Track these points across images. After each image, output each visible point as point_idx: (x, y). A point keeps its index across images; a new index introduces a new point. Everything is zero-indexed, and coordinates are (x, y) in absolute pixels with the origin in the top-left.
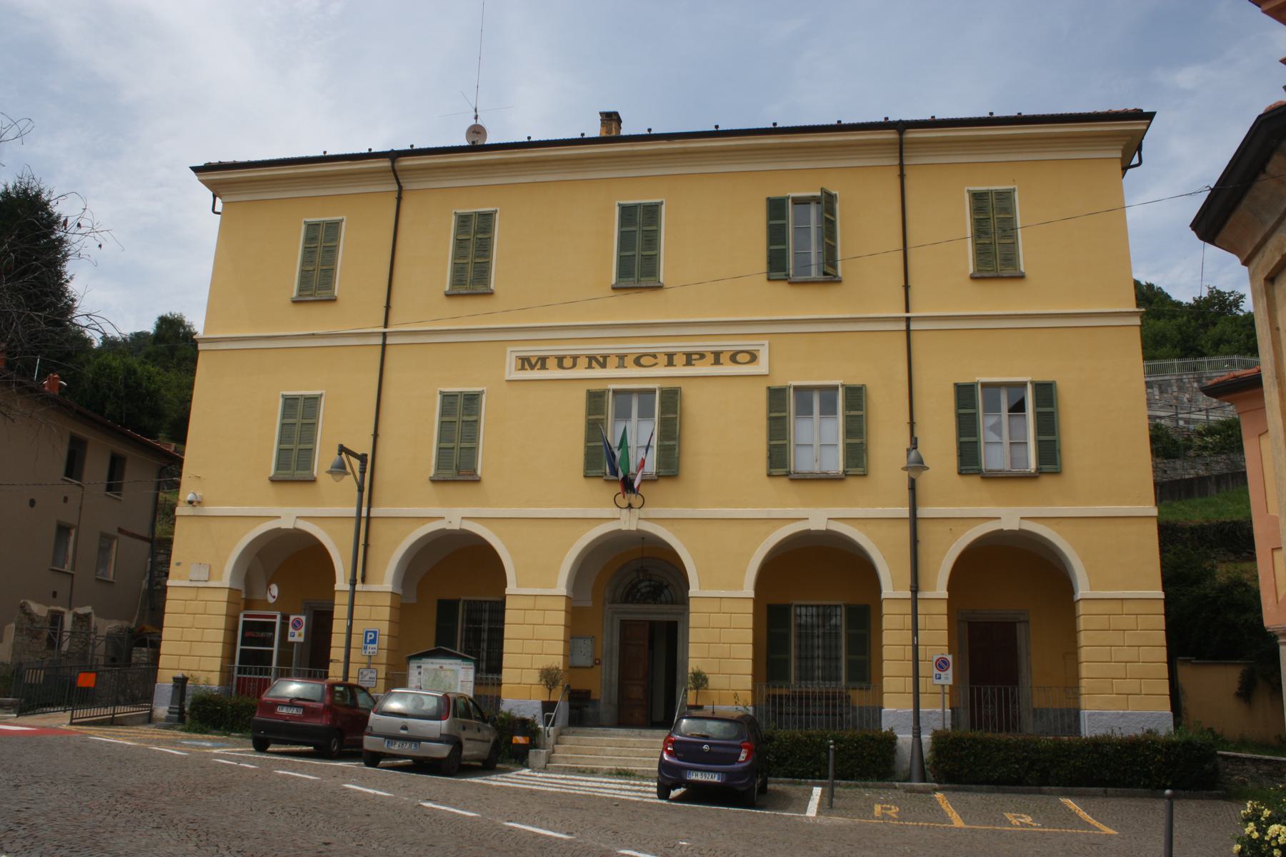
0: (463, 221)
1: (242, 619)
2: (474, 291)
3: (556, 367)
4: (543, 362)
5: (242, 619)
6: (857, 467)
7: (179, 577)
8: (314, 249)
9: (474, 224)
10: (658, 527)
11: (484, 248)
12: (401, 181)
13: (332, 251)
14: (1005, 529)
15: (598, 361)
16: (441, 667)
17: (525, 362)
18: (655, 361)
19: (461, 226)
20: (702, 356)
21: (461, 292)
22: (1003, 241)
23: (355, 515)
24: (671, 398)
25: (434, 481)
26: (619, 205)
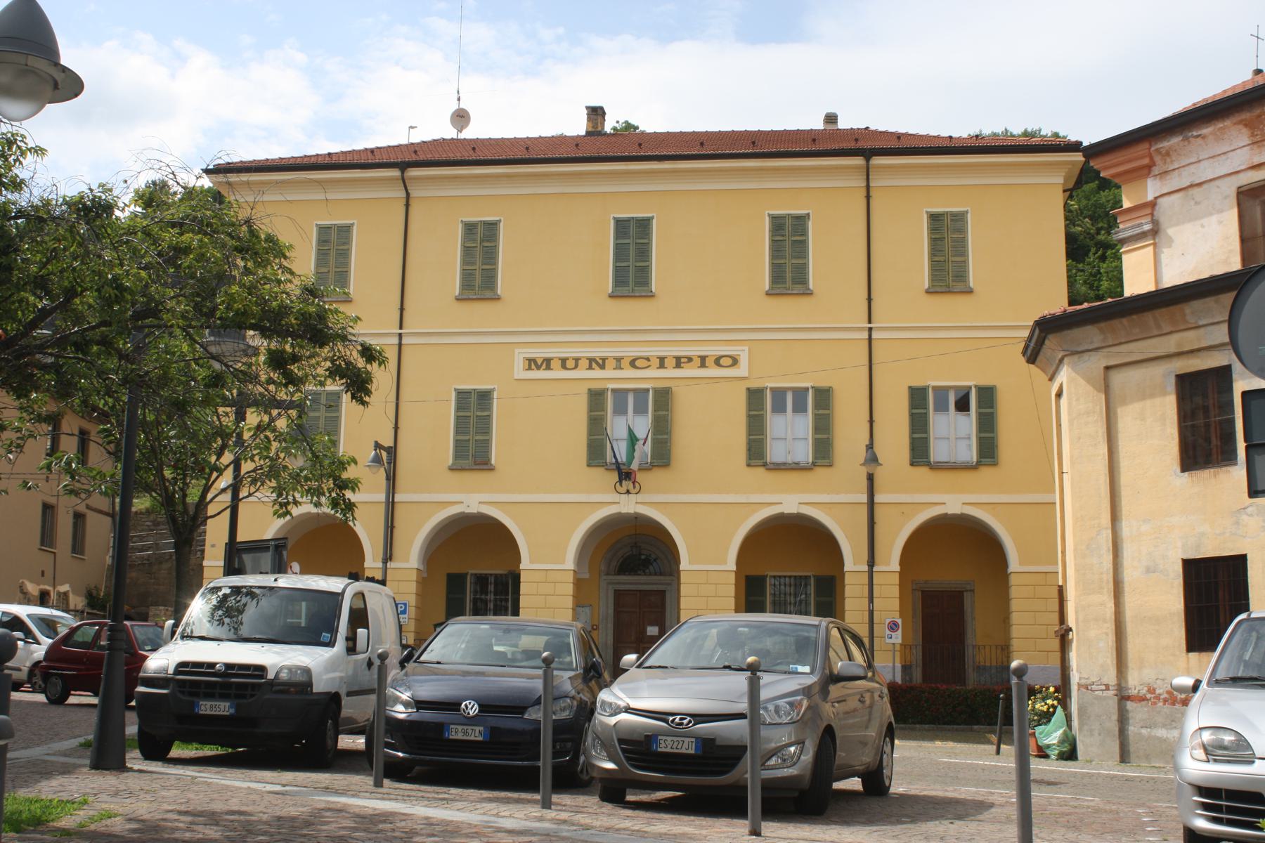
0: (469, 229)
2: (482, 297)
4: (547, 363)
6: (824, 458)
11: (490, 256)
14: (949, 513)
15: (597, 363)
17: (532, 363)
18: (649, 363)
20: (690, 359)
21: (471, 297)
22: (954, 259)
24: (664, 397)
25: (451, 469)
26: (614, 218)
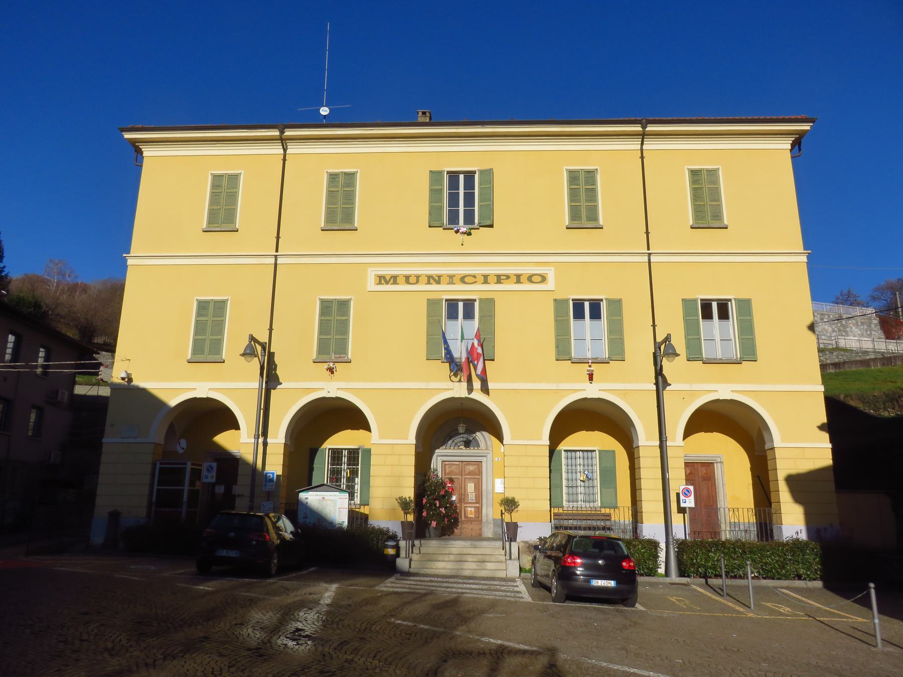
0: (333, 178)
4: (394, 279)
8: (220, 194)
9: (341, 180)
10: (740, 395)
16: (323, 498)
17: (382, 279)
18: (475, 280)
19: (332, 182)
20: (508, 277)
22: (712, 203)
24: (489, 304)
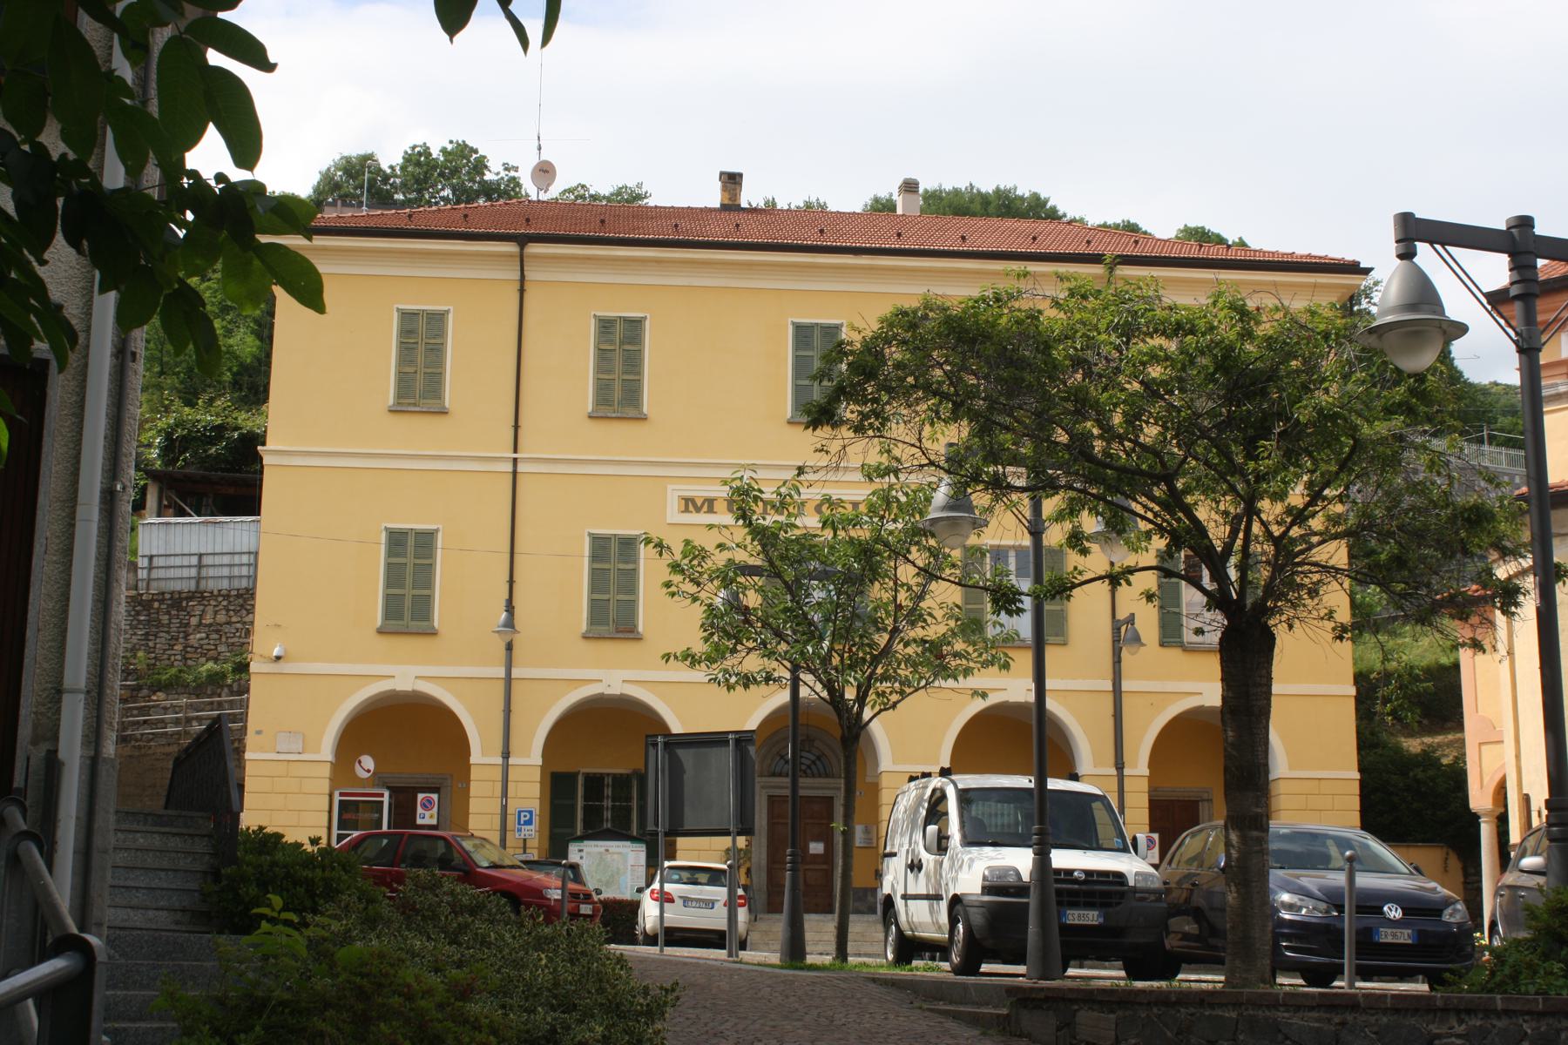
0: (604, 327)
1: (337, 798)
2: (625, 415)
3: (726, 510)
5: (337, 798)
6: (1057, 635)
7: (262, 749)
8: (415, 346)
9: (618, 329)
11: (633, 363)
12: (525, 268)
13: (438, 350)
15: (773, 507)
16: (607, 850)
17: (689, 504)
19: (603, 333)
21: (609, 415)
23: (504, 676)
25: (585, 637)
26: (793, 323)
